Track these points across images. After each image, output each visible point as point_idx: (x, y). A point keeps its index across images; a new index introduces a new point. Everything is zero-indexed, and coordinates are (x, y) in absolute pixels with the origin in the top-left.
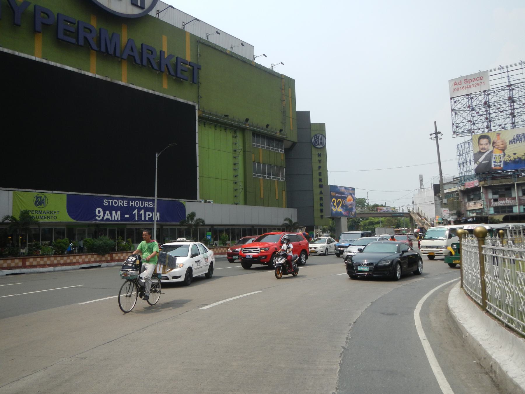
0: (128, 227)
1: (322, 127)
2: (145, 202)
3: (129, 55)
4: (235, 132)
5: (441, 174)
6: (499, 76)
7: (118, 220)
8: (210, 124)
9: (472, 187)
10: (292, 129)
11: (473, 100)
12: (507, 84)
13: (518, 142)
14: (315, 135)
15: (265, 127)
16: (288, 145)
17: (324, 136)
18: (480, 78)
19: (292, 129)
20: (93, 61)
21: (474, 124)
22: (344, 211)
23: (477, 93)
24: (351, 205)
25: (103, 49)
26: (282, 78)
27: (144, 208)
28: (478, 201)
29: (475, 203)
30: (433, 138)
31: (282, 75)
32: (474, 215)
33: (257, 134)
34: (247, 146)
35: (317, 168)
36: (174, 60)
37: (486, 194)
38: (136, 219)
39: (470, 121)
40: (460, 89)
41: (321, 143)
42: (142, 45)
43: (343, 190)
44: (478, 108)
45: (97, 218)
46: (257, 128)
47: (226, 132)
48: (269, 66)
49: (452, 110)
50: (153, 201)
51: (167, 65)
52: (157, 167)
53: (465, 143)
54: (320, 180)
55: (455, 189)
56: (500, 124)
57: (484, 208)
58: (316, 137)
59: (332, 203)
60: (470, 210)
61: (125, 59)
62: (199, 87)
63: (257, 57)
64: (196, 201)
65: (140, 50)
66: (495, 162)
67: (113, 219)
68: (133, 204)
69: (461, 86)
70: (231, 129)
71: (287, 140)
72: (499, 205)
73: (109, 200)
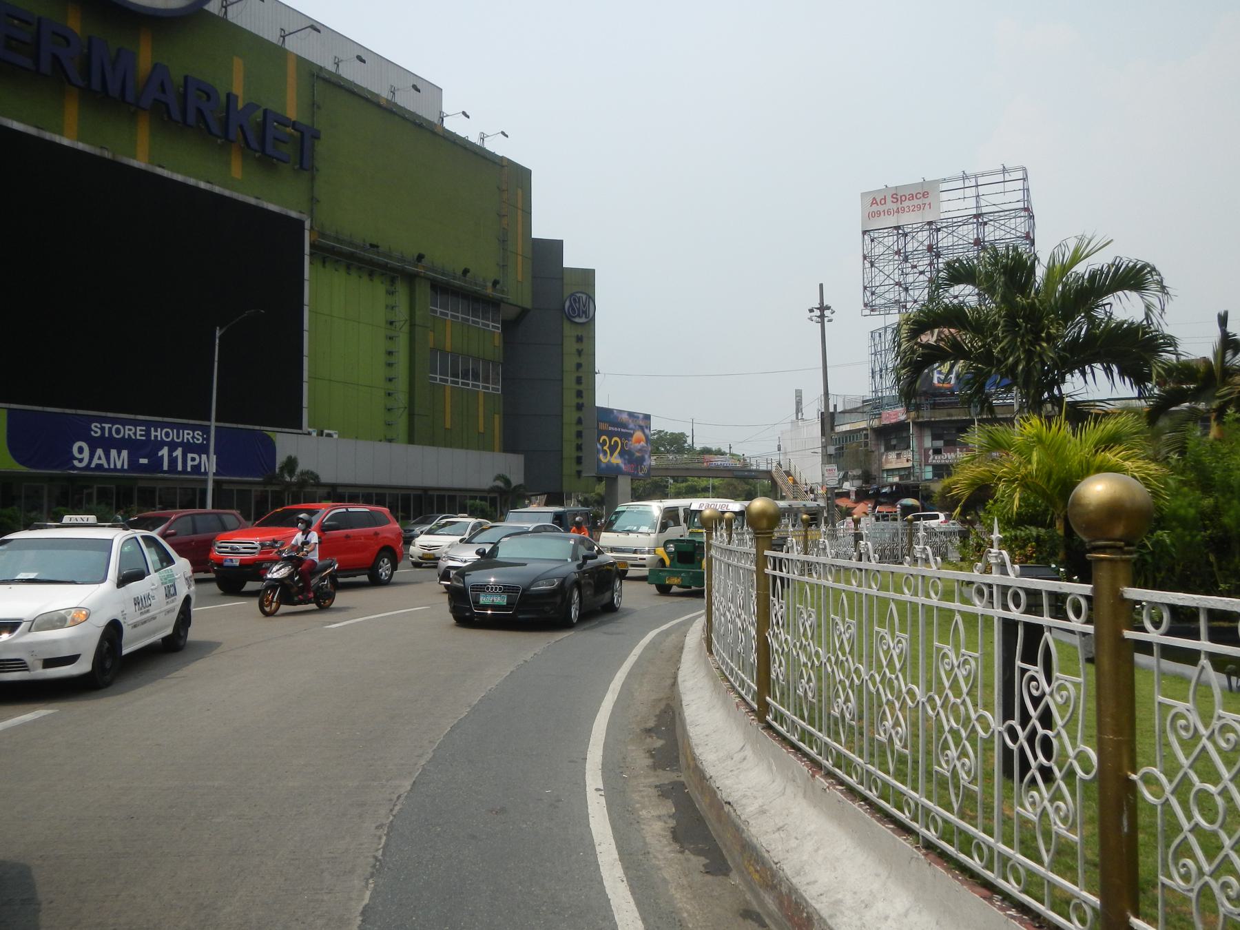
0: (142, 484)
1: (587, 277)
2: (186, 432)
3: (155, 100)
4: (393, 281)
5: (826, 393)
6: (960, 193)
7: (122, 470)
8: (337, 261)
9: (893, 421)
10: (520, 278)
11: (908, 238)
12: (974, 212)
14: (572, 295)
15: (459, 272)
16: (511, 313)
17: (591, 298)
18: (923, 195)
19: (520, 278)
20: (72, 112)
21: (906, 290)
22: (625, 464)
23: (915, 226)
24: (640, 450)
25: (96, 84)
26: (503, 166)
27: (182, 444)
28: (904, 452)
29: (899, 456)
30: (814, 318)
31: (502, 157)
32: (896, 479)
33: (443, 289)
34: (418, 313)
36: (258, 116)
37: (921, 439)
38: (165, 467)
39: (898, 284)
40: (882, 214)
41: (584, 312)
42: (186, 78)
43: (625, 417)
44: (916, 256)
45: (76, 463)
46: (443, 274)
47: (371, 280)
48: (474, 139)
49: (865, 257)
51: (241, 127)
53: (886, 328)
54: (579, 394)
55: (863, 425)
56: (956, 294)
57: (913, 467)
58: (575, 300)
59: (599, 446)
60: (888, 470)
61: (144, 109)
62: (313, 179)
63: (447, 116)
65: (181, 89)
67: (112, 466)
68: (158, 434)
69: (885, 207)
70: (383, 274)
71: (507, 303)
72: (943, 461)
73: (103, 425)
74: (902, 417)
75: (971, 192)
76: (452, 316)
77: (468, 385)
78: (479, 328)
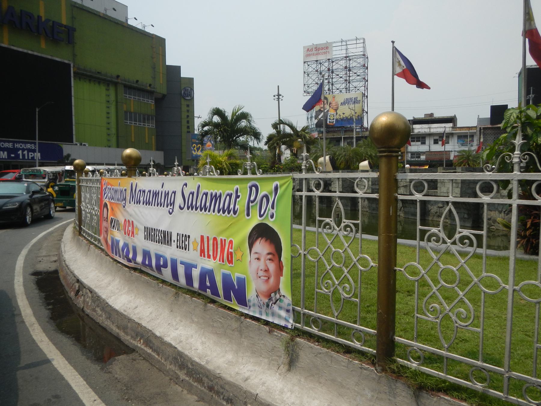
1: (190, 81)
2: (28, 145)
4: (108, 85)
6: (340, 48)
7: (5, 159)
10: (161, 83)
12: (345, 55)
13: (347, 104)
14: (185, 88)
15: (135, 81)
17: (192, 89)
19: (161, 83)
26: (153, 38)
27: (27, 149)
31: (153, 35)
35: (186, 117)
36: (51, 24)
38: (21, 157)
40: (311, 55)
41: (190, 95)
42: (21, 11)
46: (129, 82)
47: (99, 85)
48: (140, 27)
50: (35, 143)
51: (44, 29)
52: (37, 119)
54: (188, 127)
58: (186, 90)
59: (192, 148)
64: (72, 144)
66: (330, 119)
68: (18, 146)
69: (312, 52)
74: (316, 136)
75: (344, 47)
76: (133, 98)
77: (141, 124)
78: (145, 103)
